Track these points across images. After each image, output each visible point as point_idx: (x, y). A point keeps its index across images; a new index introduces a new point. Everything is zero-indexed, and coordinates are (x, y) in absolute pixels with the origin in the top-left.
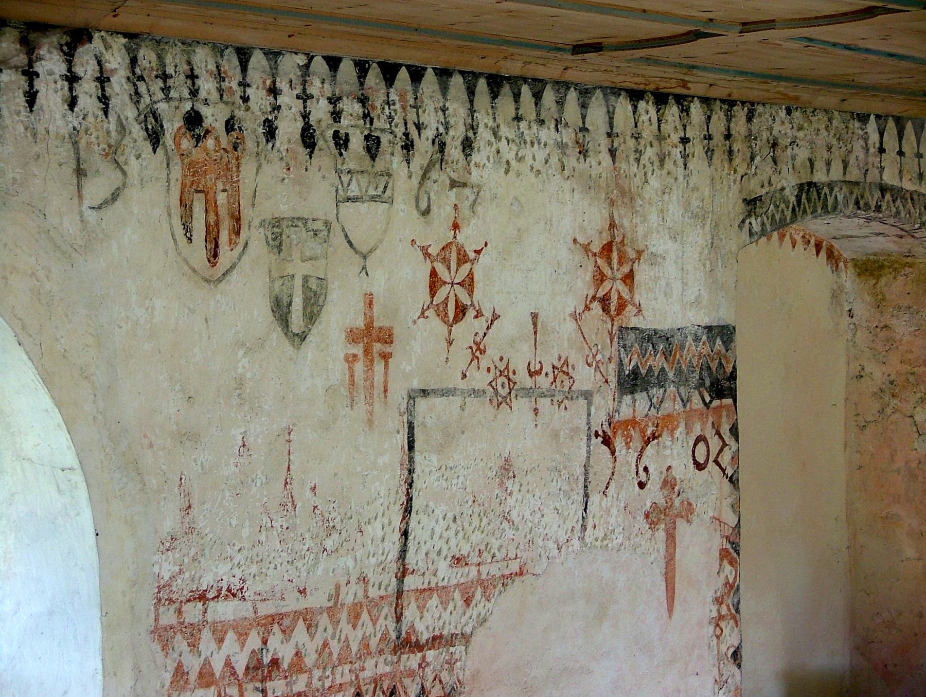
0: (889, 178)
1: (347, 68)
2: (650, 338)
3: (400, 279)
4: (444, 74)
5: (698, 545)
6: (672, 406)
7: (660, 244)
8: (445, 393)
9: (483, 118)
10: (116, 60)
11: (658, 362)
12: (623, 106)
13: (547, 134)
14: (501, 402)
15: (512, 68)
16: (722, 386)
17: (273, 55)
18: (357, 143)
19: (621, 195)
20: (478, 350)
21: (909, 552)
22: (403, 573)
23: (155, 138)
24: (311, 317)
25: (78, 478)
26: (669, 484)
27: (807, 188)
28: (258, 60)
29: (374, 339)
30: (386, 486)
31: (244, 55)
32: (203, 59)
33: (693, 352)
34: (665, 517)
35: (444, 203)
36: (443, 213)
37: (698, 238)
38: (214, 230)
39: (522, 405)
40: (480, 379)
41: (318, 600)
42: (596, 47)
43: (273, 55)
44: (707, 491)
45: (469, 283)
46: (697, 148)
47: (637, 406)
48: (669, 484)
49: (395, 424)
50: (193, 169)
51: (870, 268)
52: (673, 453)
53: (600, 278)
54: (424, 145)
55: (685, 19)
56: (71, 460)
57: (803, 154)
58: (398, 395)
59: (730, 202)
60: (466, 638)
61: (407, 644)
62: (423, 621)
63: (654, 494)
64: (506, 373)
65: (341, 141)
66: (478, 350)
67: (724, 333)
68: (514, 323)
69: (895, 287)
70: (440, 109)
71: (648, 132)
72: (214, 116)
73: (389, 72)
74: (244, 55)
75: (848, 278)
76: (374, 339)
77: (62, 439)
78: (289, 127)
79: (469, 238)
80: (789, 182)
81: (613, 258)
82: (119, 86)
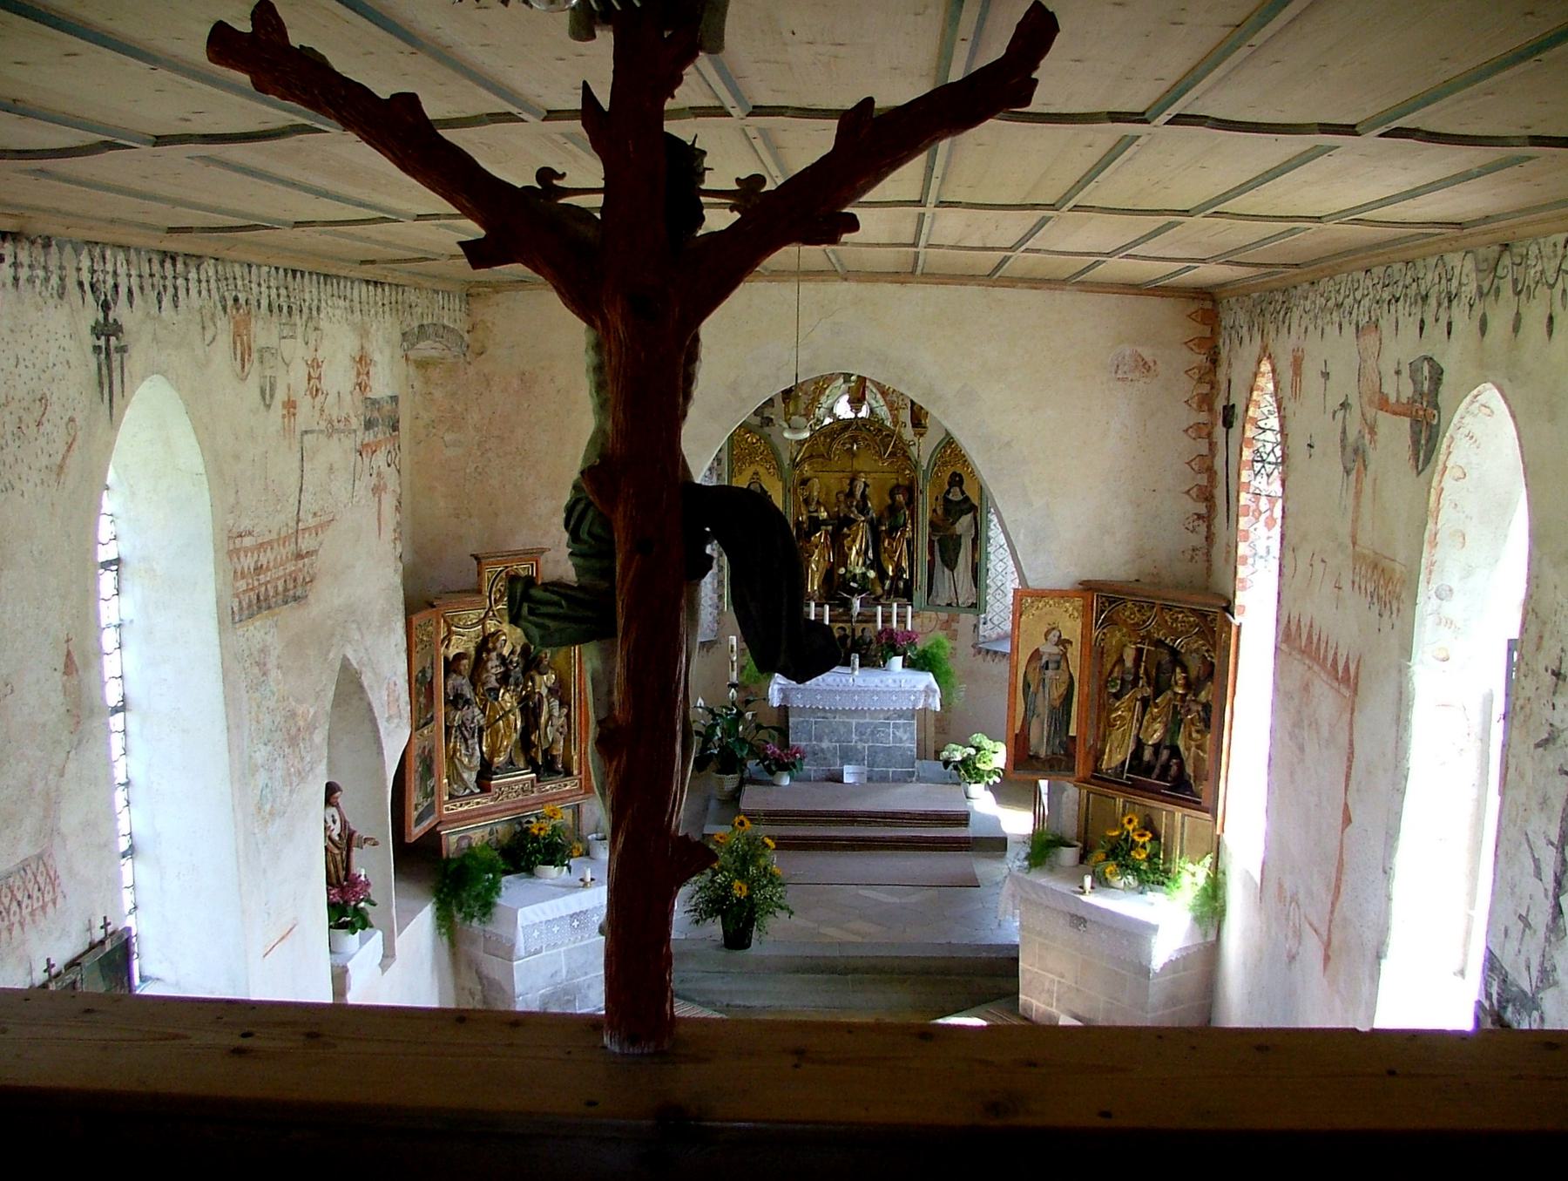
0: (446, 322)
1: (281, 271)
2: (374, 402)
3: (299, 373)
4: (310, 273)
5: (389, 501)
6: (380, 436)
7: (377, 357)
8: (312, 432)
9: (323, 296)
10: (211, 272)
11: (376, 414)
12: (364, 286)
13: (341, 303)
14: (330, 436)
15: (333, 271)
16: (395, 428)
17: (259, 266)
18: (285, 309)
19: (364, 333)
20: (322, 410)
21: (442, 504)
22: (298, 521)
23: (224, 309)
24: (272, 396)
25: (204, 478)
26: (379, 474)
27: (421, 326)
28: (254, 269)
29: (290, 405)
30: (294, 479)
31: (249, 266)
32: (237, 268)
33: (387, 407)
34: (377, 490)
35: (312, 336)
36: (312, 343)
37: (387, 352)
38: (243, 352)
39: (335, 436)
40: (323, 425)
41: (274, 536)
42: (373, 262)
43: (259, 266)
44: (390, 474)
45: (319, 378)
46: (387, 308)
47: (369, 437)
48: (379, 474)
49: (297, 448)
50: (236, 324)
51: (423, 365)
52: (380, 459)
53: (359, 374)
54: (305, 310)
55: (409, 249)
56: (201, 469)
57: (419, 310)
58: (298, 433)
59: (397, 337)
60: (316, 551)
61: (299, 556)
62: (306, 544)
63: (374, 480)
64: (330, 422)
65: (280, 308)
66: (322, 410)
67: (394, 399)
68: (331, 399)
69: (435, 374)
70: (309, 291)
71: (372, 301)
72: (242, 297)
73: (294, 272)
74: (249, 266)
75: (412, 370)
76: (290, 405)
77: (200, 459)
78: (264, 303)
79: (320, 356)
80: (415, 324)
81: (363, 361)
82: (213, 284)
